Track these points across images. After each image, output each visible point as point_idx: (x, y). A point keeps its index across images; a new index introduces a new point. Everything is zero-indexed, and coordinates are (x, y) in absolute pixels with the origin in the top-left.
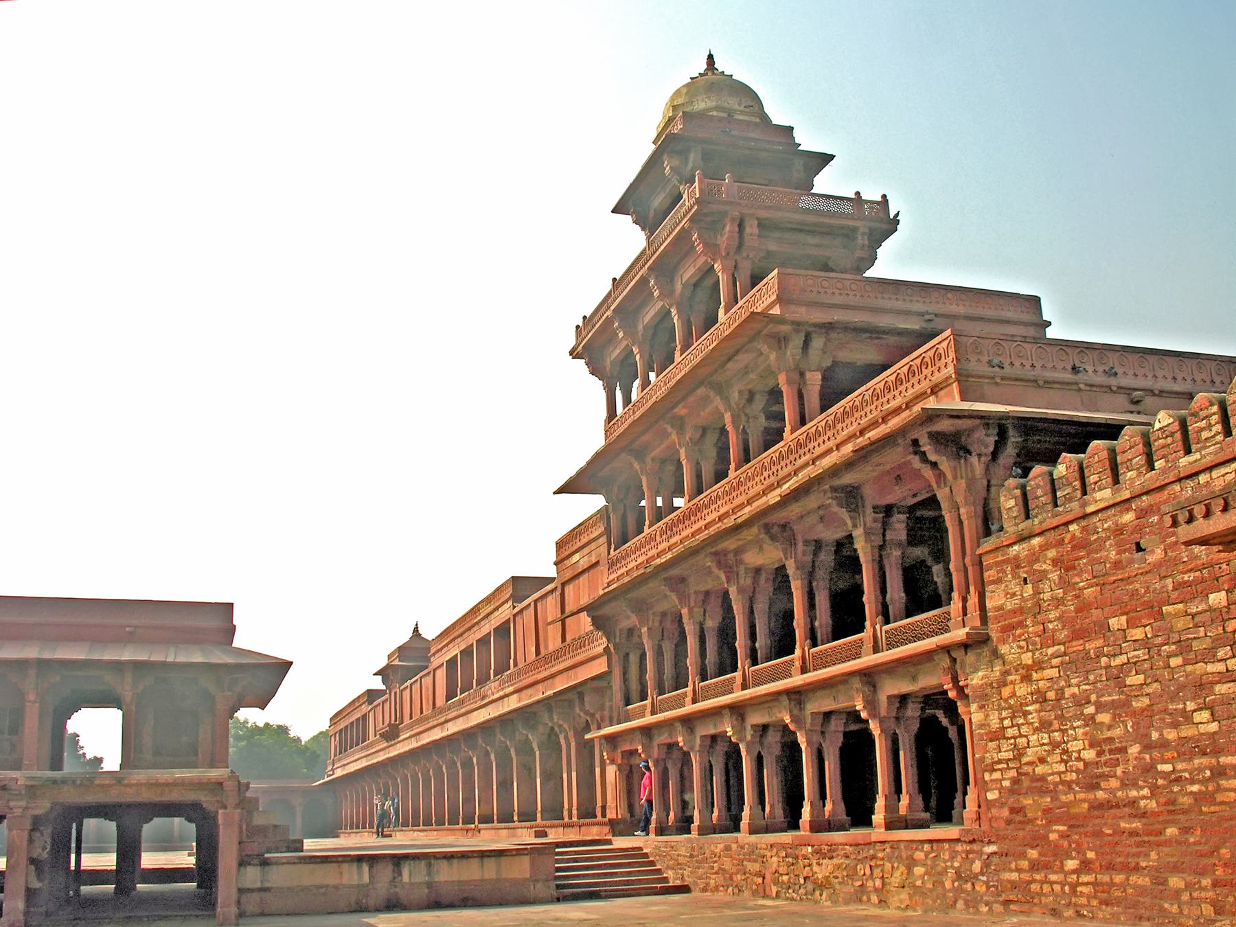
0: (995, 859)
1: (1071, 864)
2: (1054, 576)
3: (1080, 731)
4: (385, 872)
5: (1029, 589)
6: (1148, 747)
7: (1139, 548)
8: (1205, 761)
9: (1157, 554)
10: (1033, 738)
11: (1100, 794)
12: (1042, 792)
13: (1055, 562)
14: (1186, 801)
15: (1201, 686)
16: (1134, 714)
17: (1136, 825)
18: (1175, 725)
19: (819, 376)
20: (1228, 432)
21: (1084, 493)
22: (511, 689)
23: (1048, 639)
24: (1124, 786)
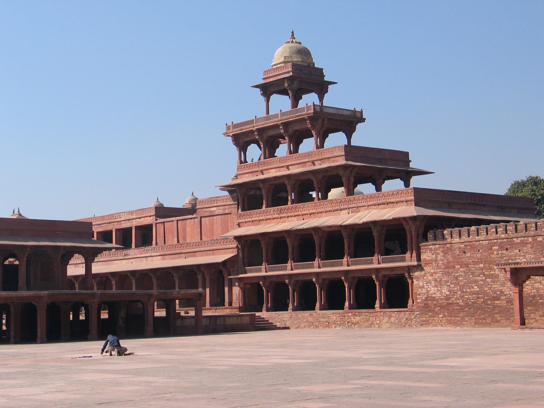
0: (418, 315)
1: (441, 316)
2: (442, 254)
3: (446, 288)
4: (239, 318)
5: (434, 256)
6: (463, 292)
7: (464, 252)
8: (475, 296)
9: (469, 254)
10: (432, 289)
11: (450, 301)
12: (434, 300)
13: (442, 251)
14: (470, 303)
15: (476, 282)
16: (460, 285)
17: (458, 308)
18: (470, 288)
19: (353, 178)
20: (487, 234)
21: (452, 238)
22: (158, 254)
23: (438, 267)
24: (456, 300)
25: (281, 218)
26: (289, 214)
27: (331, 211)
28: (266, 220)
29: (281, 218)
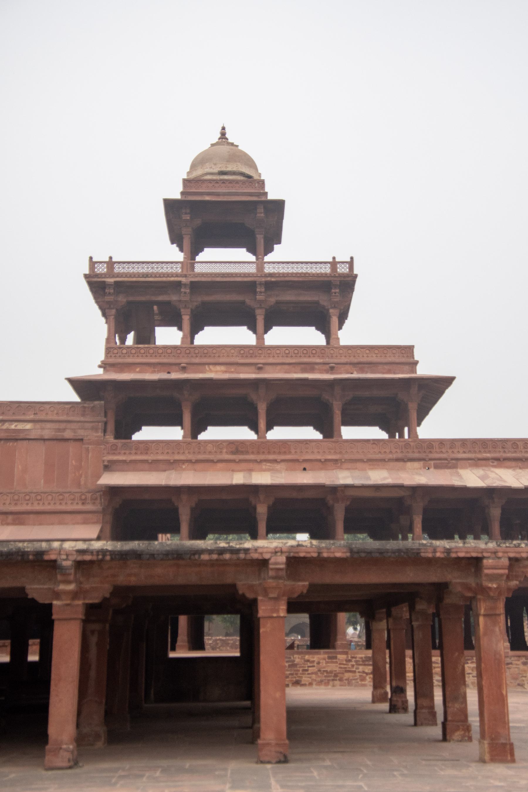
25: (241, 461)
26: (262, 457)
27: (383, 460)
28: (198, 461)
29: (241, 461)
